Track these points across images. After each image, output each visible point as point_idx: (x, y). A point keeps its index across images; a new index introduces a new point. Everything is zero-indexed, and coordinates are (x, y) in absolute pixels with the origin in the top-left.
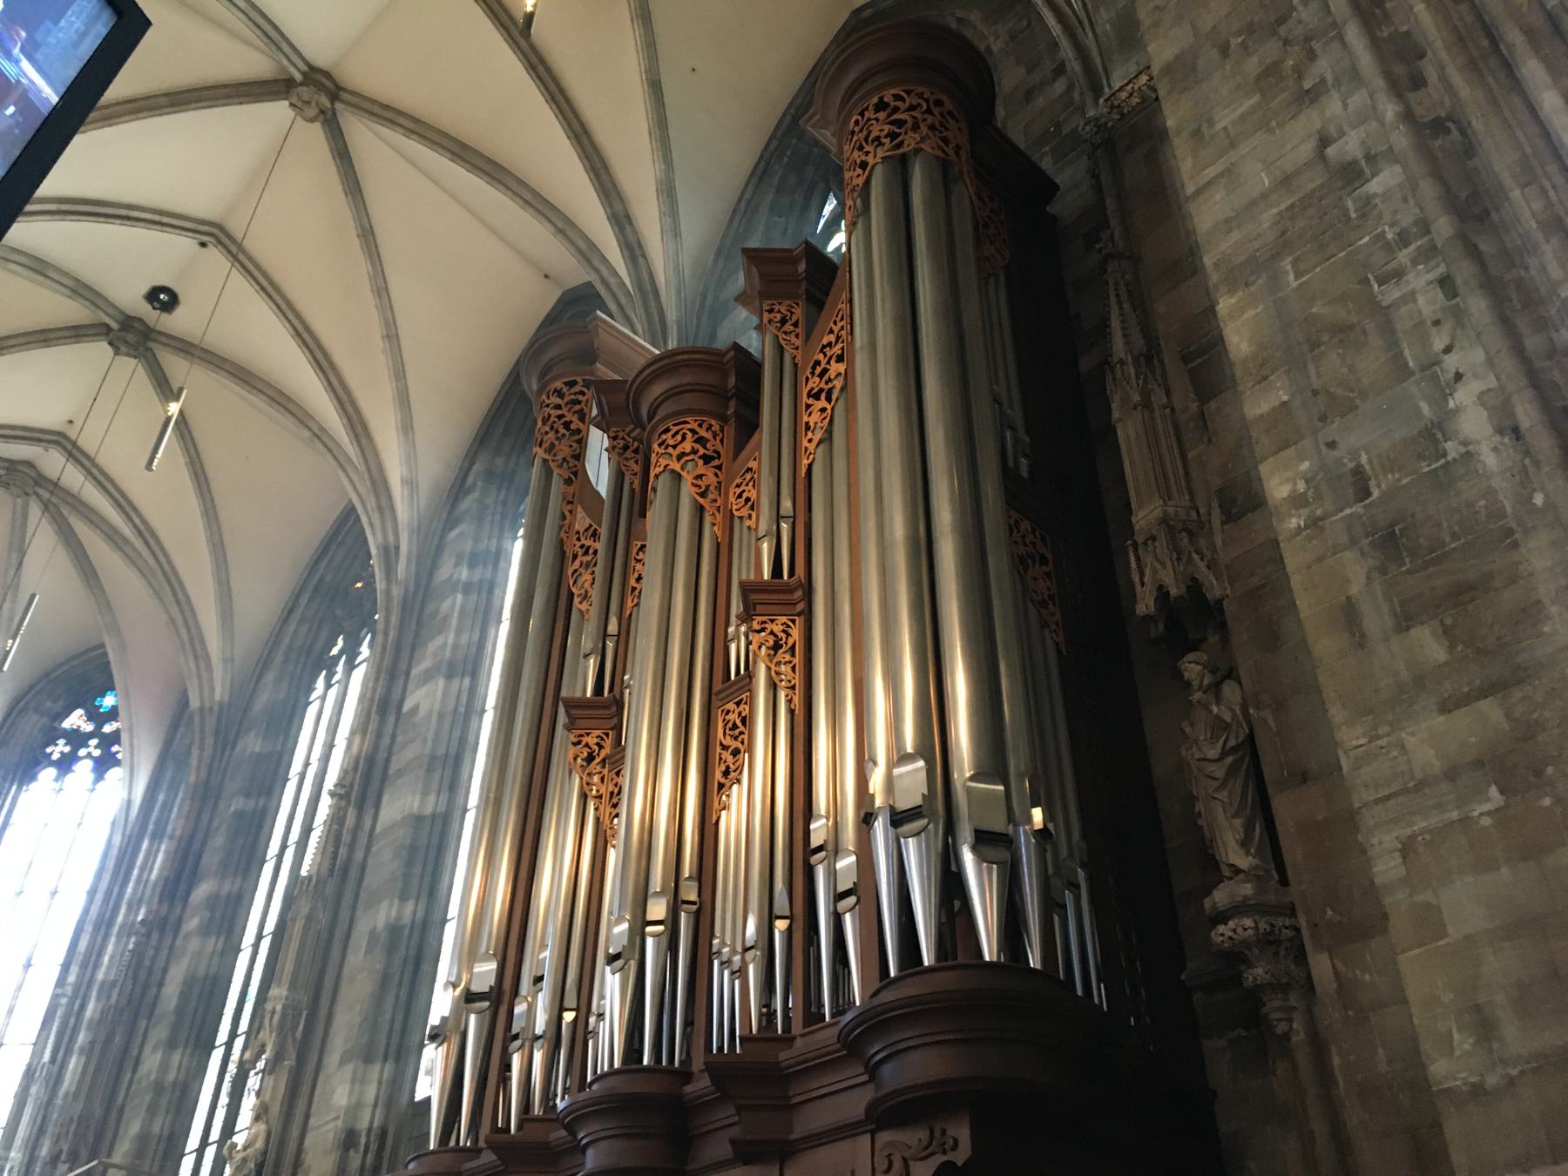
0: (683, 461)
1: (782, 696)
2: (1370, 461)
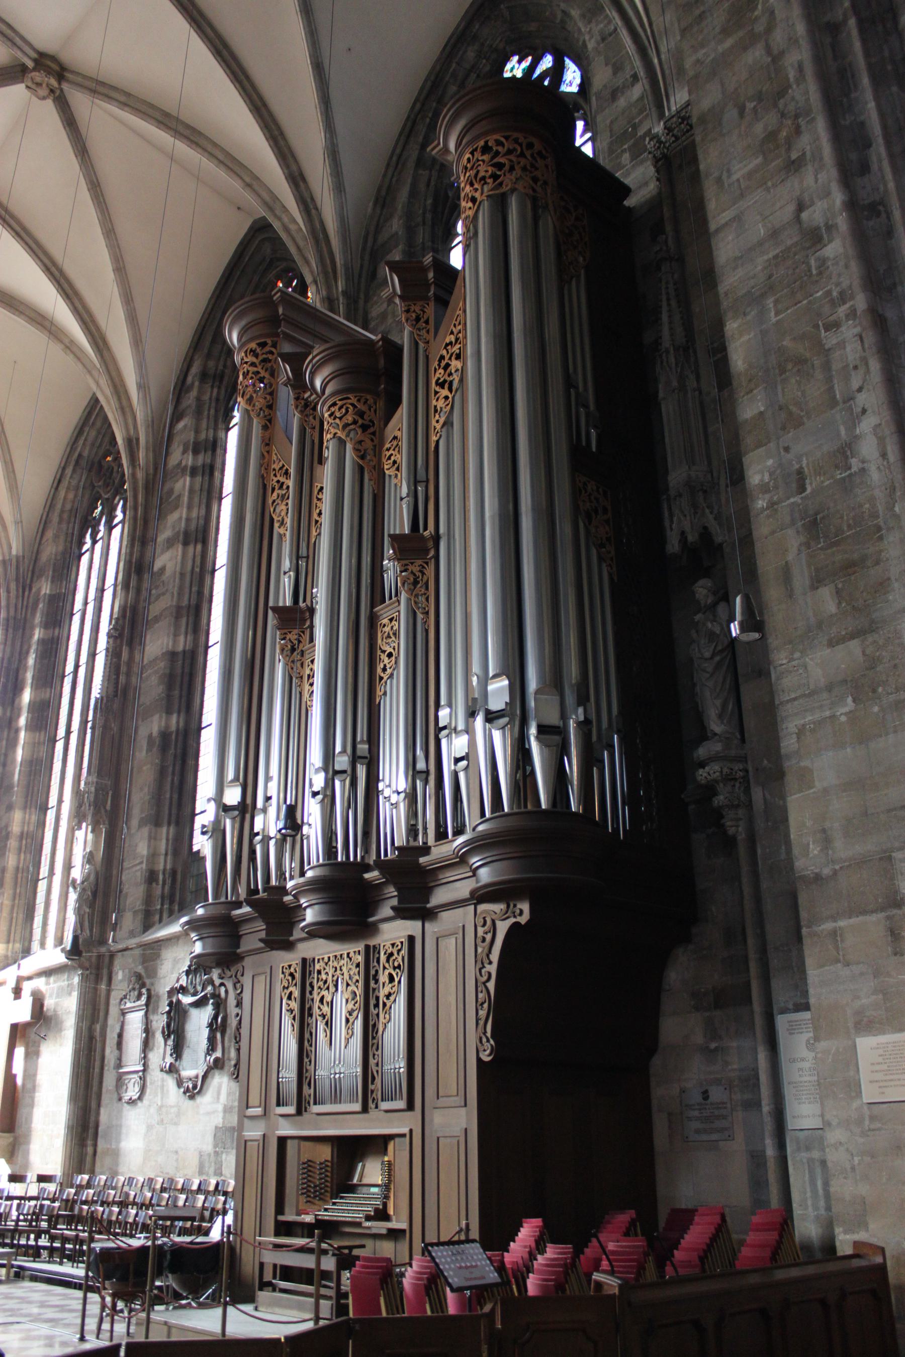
0: (348, 429)
2: (808, 464)
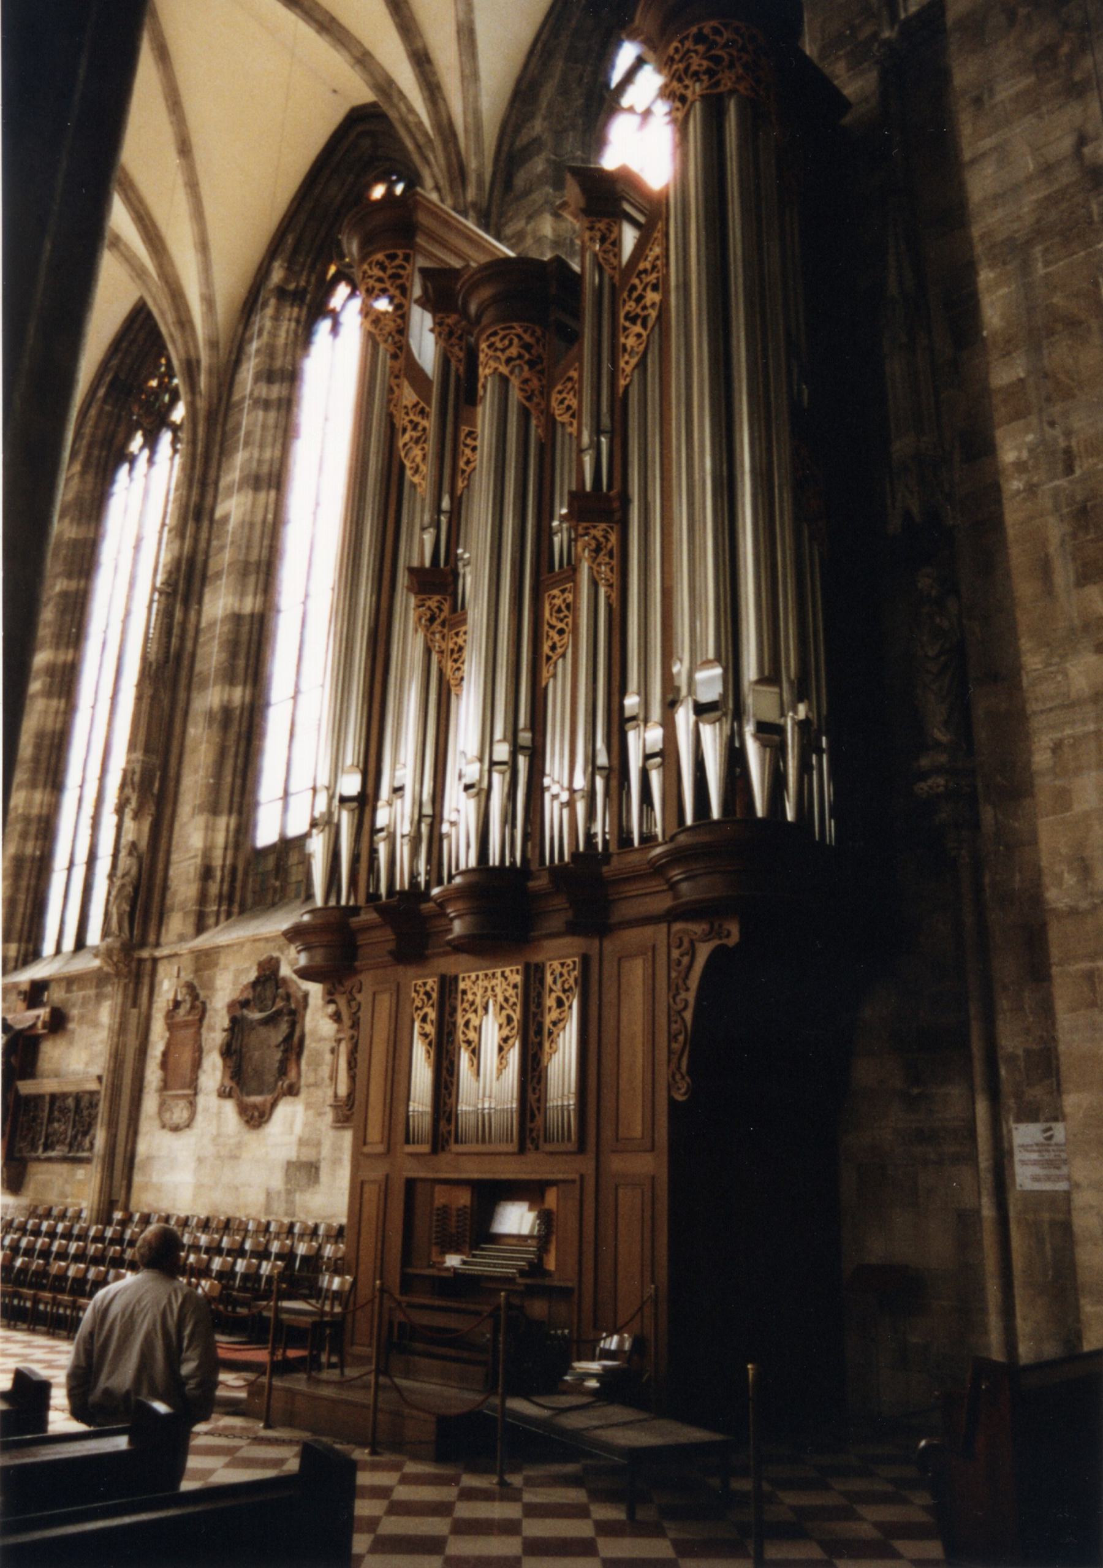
0: (513, 363)
1: (602, 591)
